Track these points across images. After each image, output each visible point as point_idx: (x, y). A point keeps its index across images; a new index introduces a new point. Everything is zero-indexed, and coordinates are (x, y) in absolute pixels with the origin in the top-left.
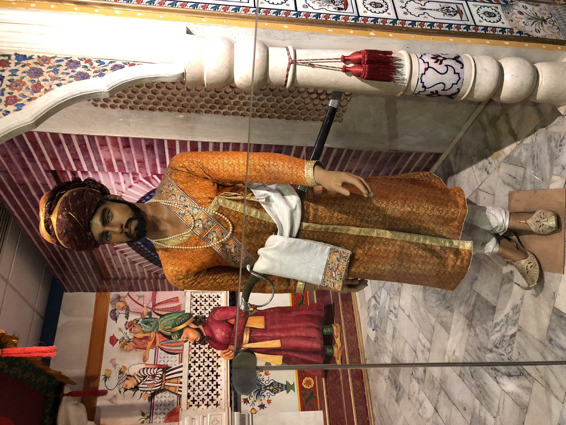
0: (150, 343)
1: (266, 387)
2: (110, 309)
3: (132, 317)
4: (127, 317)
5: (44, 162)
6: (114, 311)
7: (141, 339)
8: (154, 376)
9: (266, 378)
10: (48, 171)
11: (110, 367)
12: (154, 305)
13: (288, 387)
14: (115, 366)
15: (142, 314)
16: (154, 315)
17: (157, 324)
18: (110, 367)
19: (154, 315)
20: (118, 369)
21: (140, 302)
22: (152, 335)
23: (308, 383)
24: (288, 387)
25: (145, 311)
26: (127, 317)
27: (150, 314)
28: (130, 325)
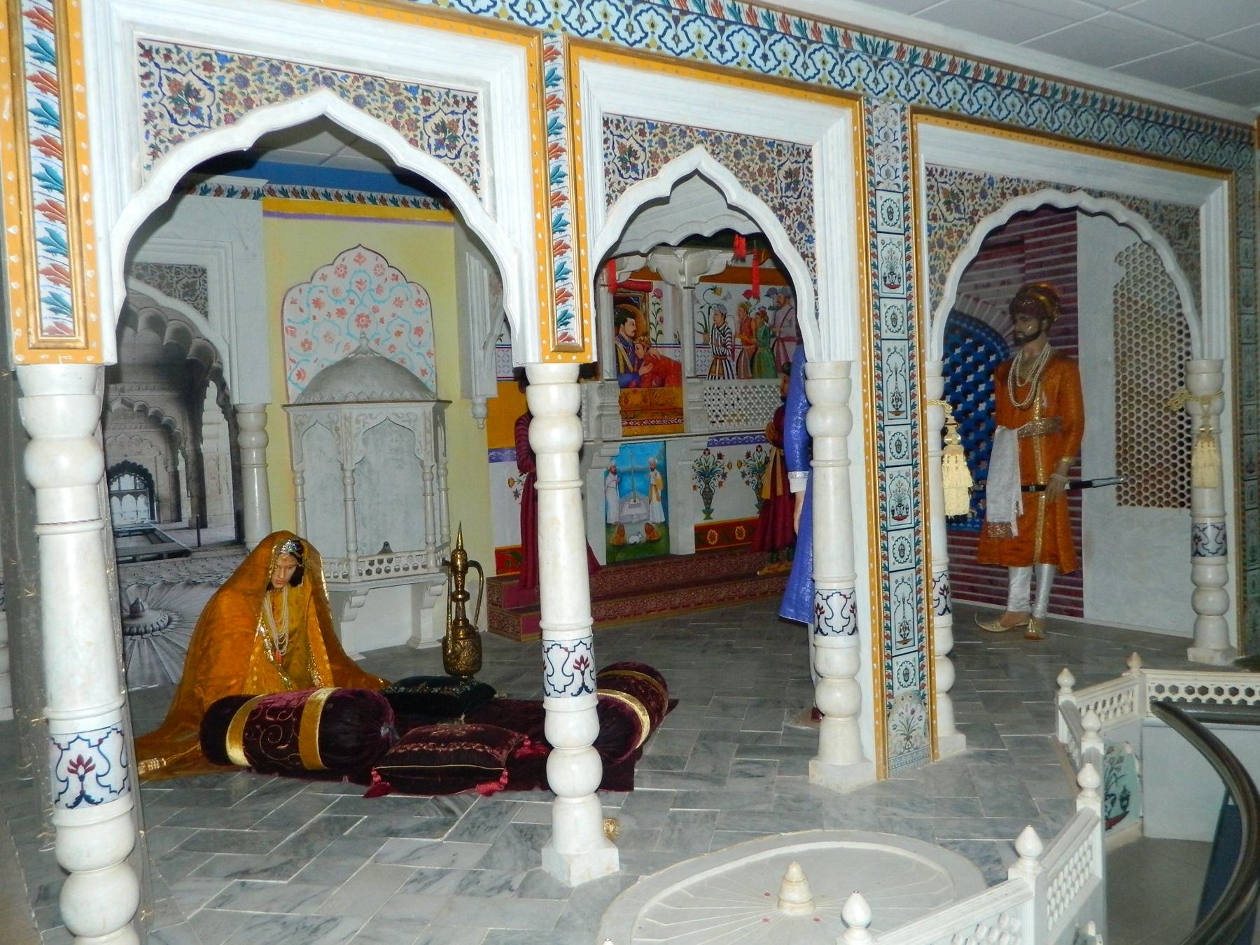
0: (746, 338)
1: (707, 483)
2: (778, 288)
3: (770, 314)
4: (770, 308)
5: (1035, 235)
6: (775, 291)
7: (750, 326)
8: (724, 346)
9: (716, 483)
10: (1023, 237)
11: (724, 294)
12: (783, 340)
13: (708, 512)
14: (725, 299)
15: (773, 326)
16: (773, 340)
17: (764, 346)
18: (724, 294)
19: (773, 340)
20: (723, 302)
21: (786, 323)
22: (754, 340)
23: (712, 538)
24: (708, 512)
25: (776, 330)
26: (770, 308)
27: (774, 336)
28: (763, 314)
